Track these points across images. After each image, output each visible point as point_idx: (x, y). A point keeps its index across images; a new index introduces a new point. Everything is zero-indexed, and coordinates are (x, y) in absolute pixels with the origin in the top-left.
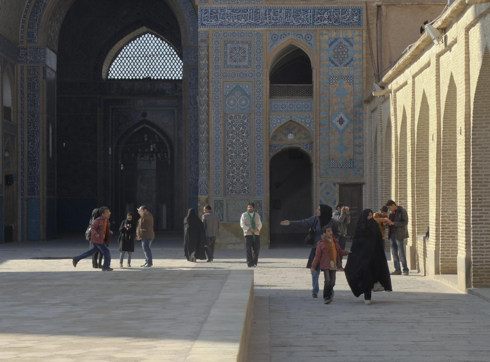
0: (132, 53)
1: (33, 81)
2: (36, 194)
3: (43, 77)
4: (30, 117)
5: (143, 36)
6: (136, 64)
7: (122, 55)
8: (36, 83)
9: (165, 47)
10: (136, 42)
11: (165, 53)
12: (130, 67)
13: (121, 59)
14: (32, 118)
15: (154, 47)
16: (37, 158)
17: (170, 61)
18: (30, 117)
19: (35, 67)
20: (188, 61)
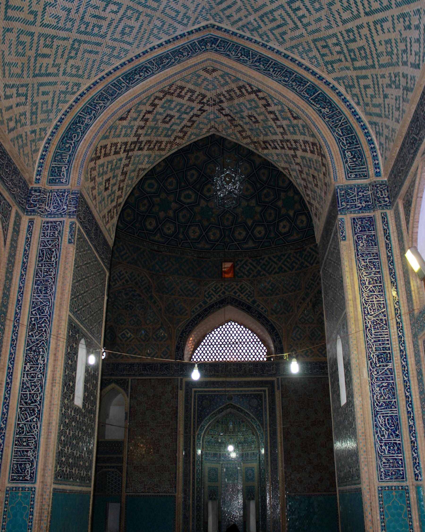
0: (215, 341)
1: (50, 247)
2: (29, 478)
3: (70, 239)
4: (34, 313)
5: (226, 324)
6: (219, 351)
7: (204, 343)
8: (53, 250)
9: (248, 335)
10: (219, 330)
11: (248, 340)
12: (213, 354)
13: (204, 347)
14: (38, 316)
15: (237, 335)
16: (39, 398)
17: (254, 348)
18: (34, 313)
19: (55, 222)
20: (348, 207)
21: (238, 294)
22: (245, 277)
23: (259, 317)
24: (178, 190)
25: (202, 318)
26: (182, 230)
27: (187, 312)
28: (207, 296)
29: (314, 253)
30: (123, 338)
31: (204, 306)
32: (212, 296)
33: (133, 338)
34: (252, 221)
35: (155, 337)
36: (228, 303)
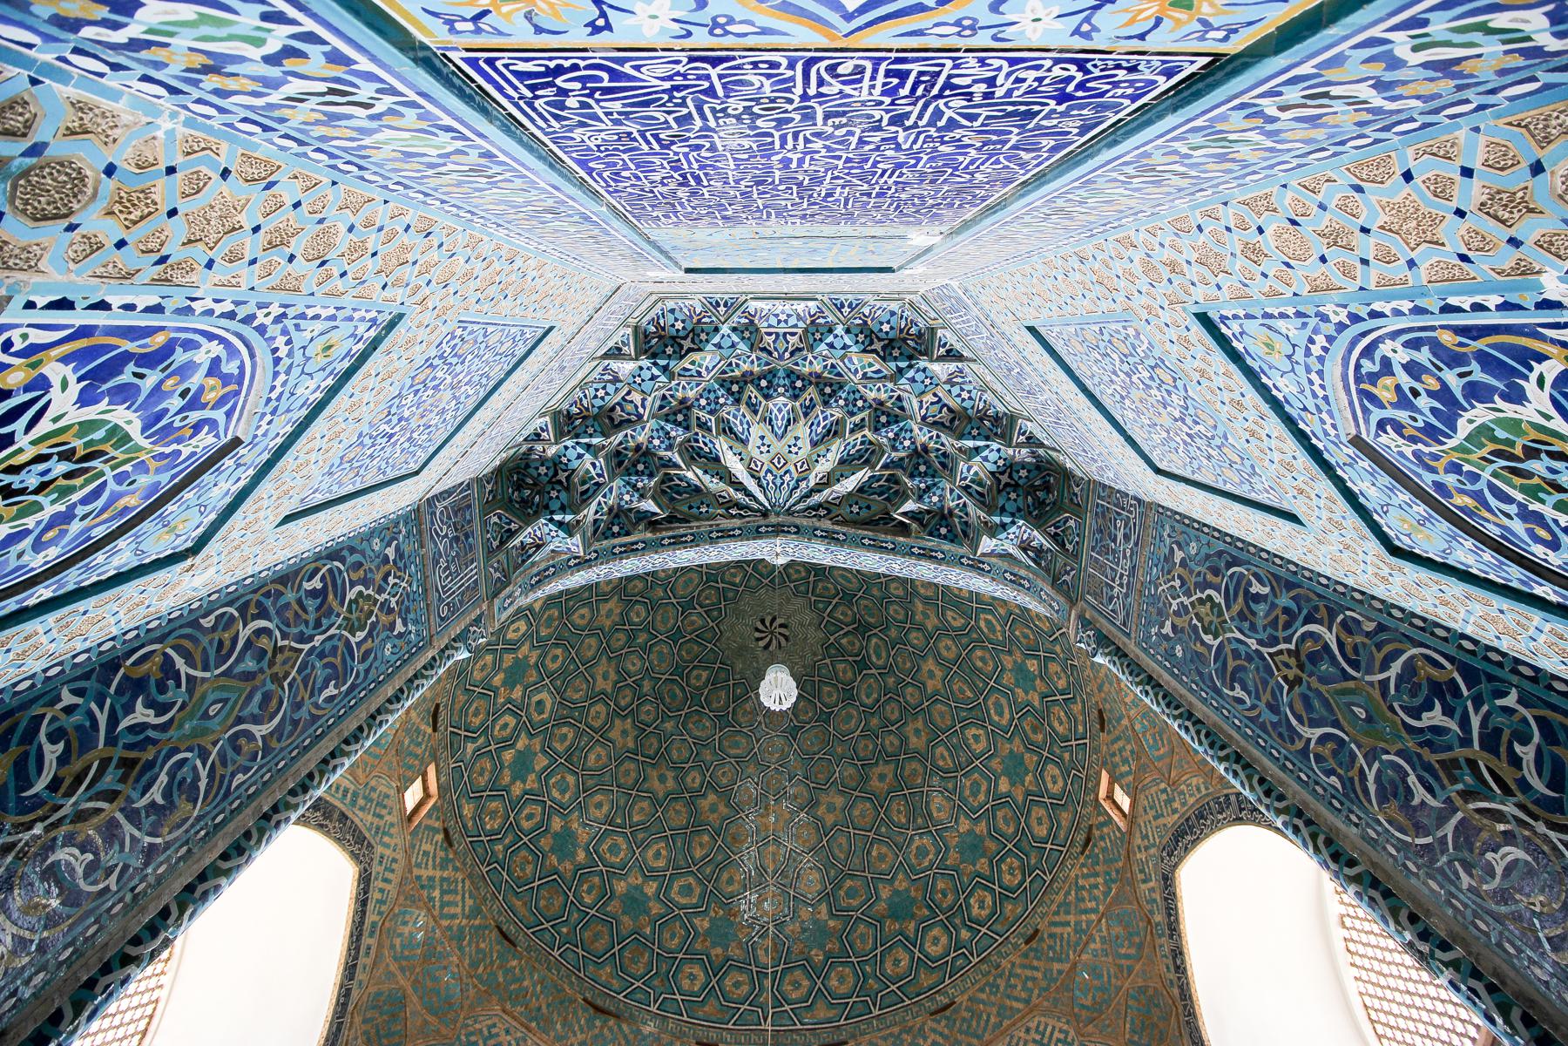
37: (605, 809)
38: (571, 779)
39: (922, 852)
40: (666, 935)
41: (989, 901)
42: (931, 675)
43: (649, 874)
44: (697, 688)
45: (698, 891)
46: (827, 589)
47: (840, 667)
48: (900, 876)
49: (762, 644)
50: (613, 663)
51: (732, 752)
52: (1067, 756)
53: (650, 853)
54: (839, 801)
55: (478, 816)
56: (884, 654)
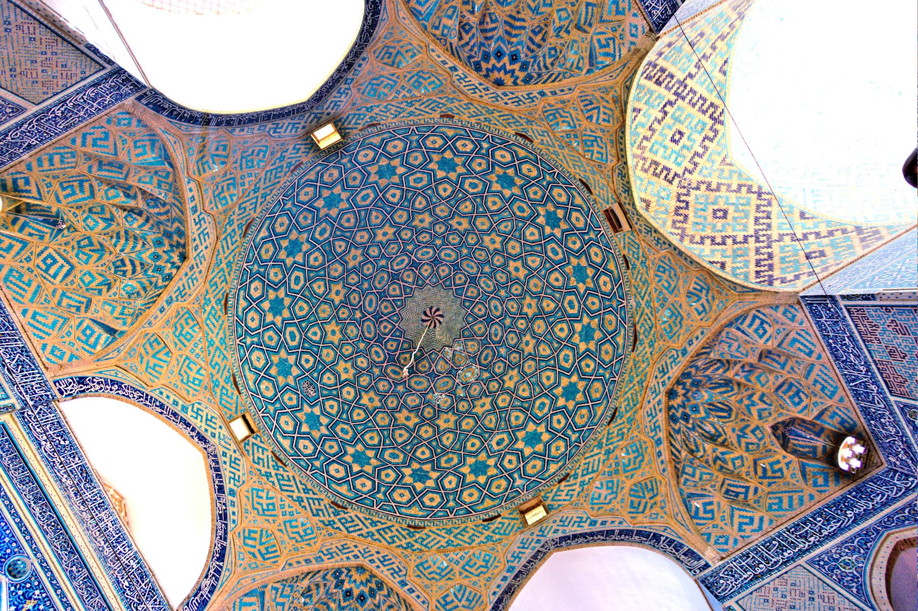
21: (225, 459)
22: (251, 458)
23: (220, 515)
24: (296, 321)
25: (161, 413)
26: (256, 339)
27: (156, 380)
28: (195, 410)
29: (360, 523)
30: (44, 261)
31: (179, 408)
32: (199, 418)
33: (53, 283)
34: (308, 430)
35: (85, 325)
36: (205, 449)
37: (549, 373)
38: (538, 403)
39: (474, 186)
40: (594, 308)
41: (459, 144)
42: (385, 234)
43: (572, 331)
44: (479, 344)
45: (569, 298)
46: (386, 307)
47: (426, 274)
48: (493, 189)
49: (441, 319)
50: (476, 403)
51: (500, 308)
52: (344, 161)
53: (563, 335)
54: (487, 239)
55: (556, 459)
56: (399, 259)
